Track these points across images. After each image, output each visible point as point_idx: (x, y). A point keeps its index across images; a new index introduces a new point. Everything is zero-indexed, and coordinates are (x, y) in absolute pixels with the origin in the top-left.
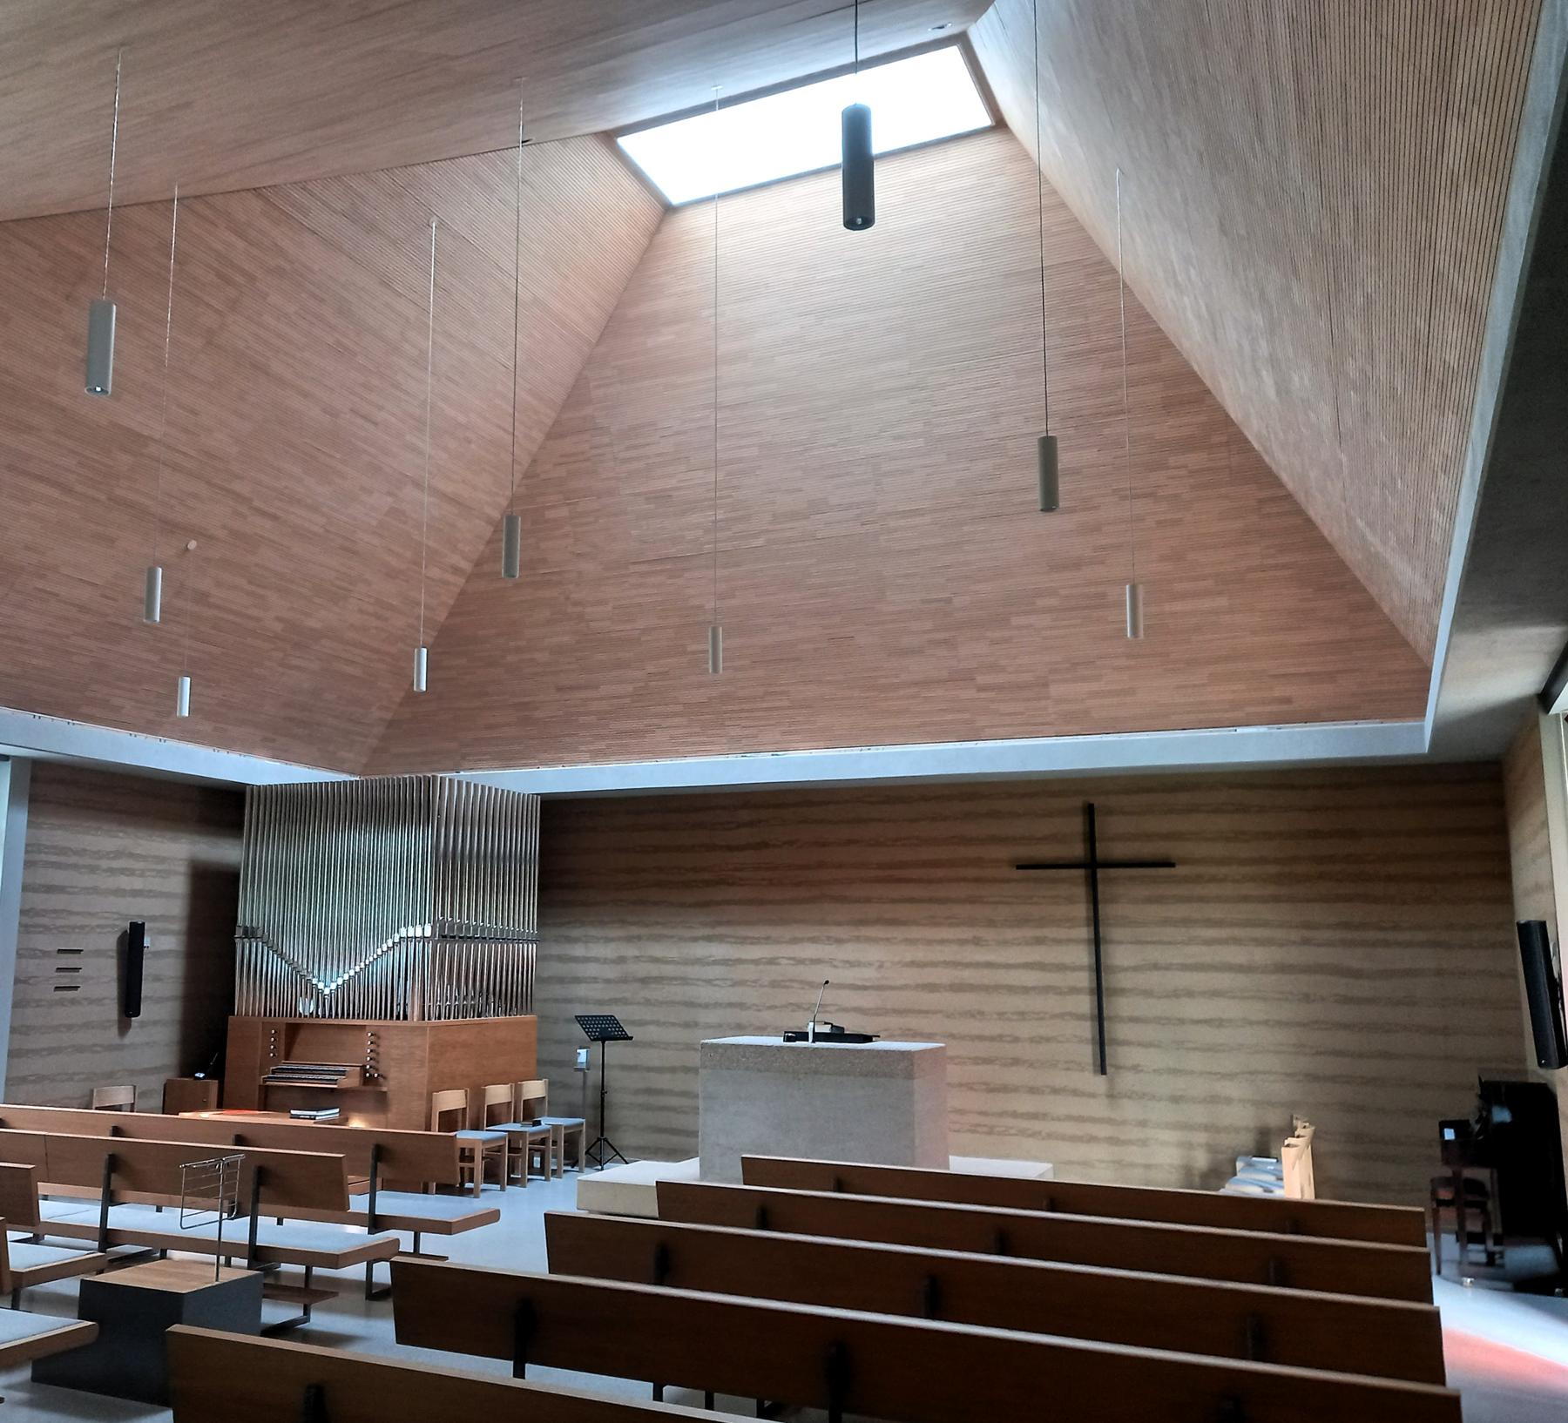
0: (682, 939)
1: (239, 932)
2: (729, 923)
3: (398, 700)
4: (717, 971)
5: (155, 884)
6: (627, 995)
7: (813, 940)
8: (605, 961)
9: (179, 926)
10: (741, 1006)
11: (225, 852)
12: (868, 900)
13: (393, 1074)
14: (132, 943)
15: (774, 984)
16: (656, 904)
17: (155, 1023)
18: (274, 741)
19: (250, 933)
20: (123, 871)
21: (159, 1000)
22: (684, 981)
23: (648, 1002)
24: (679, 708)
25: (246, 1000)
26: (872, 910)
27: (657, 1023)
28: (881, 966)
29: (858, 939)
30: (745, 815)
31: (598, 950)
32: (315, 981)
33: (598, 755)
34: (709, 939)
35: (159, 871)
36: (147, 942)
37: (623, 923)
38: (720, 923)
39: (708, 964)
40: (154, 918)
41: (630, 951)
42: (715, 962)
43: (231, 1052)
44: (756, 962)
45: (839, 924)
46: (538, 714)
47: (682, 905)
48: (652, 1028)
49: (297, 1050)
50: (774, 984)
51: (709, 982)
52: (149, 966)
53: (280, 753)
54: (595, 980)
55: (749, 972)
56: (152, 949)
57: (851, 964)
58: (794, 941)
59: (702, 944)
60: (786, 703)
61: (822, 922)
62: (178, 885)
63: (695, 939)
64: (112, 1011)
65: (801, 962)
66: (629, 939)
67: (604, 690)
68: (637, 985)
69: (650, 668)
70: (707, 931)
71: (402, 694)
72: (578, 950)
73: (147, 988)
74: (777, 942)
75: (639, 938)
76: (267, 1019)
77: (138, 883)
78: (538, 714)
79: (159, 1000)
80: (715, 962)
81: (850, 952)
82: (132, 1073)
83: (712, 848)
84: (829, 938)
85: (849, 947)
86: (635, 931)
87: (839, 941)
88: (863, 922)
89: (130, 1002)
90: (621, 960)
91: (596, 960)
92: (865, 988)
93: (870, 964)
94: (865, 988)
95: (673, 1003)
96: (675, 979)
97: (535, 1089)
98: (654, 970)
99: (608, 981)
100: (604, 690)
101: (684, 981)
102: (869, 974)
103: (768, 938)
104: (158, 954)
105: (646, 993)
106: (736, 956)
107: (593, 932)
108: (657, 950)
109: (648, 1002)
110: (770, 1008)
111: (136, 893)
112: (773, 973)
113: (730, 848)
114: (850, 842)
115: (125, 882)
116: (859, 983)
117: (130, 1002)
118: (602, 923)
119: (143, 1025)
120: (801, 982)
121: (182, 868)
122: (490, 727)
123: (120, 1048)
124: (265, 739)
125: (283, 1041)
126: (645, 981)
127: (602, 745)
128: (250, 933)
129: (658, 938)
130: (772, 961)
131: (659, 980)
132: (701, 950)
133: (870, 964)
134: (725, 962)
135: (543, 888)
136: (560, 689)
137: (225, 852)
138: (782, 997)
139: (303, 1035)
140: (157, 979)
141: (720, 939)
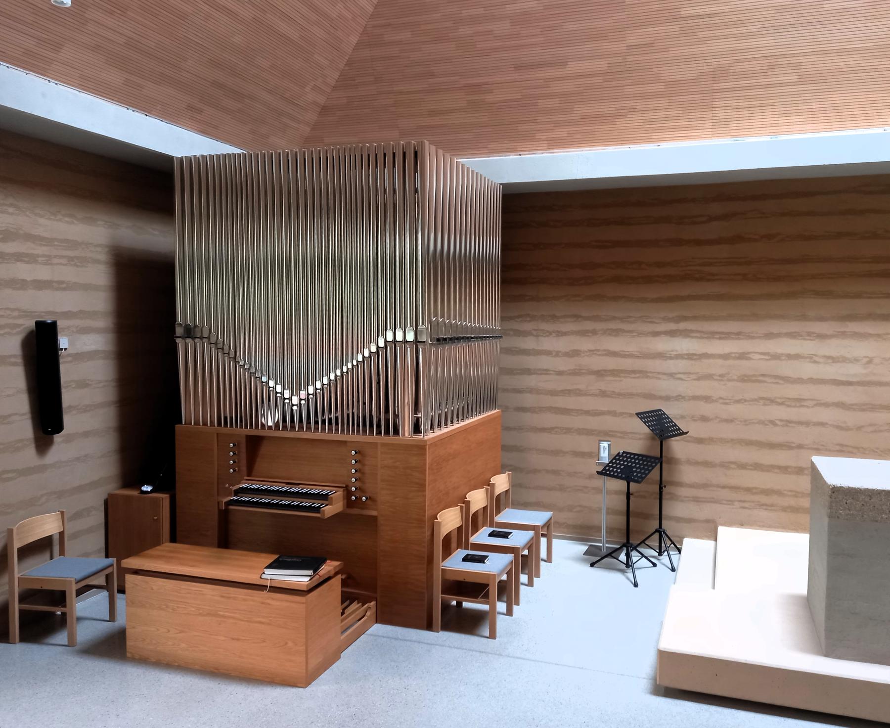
0: (641, 334)
1: (179, 331)
2: (695, 318)
3: (333, 82)
4: (680, 365)
5: (68, 274)
6: (582, 387)
7: (792, 335)
8: (557, 354)
9: (105, 322)
10: (707, 399)
11: (148, 236)
12: (858, 296)
13: (384, 496)
14: (41, 349)
15: (745, 379)
16: (615, 299)
17: (86, 434)
18: (200, 111)
19: (189, 333)
20: (19, 257)
21: (86, 409)
22: (643, 374)
23: (603, 394)
24: (661, 87)
25: (195, 407)
26: (862, 306)
27: (613, 413)
28: (870, 361)
29: (843, 335)
30: (716, 208)
31: (547, 343)
32: (264, 379)
33: (555, 144)
34: (672, 334)
35: (71, 259)
36: (63, 342)
37: (577, 317)
38: (685, 319)
39: (671, 358)
40: (68, 315)
41: (584, 344)
42: (680, 357)
43: (181, 463)
44: (726, 357)
45: (822, 319)
46: (489, 98)
47: (643, 300)
48: (608, 418)
49: (261, 465)
50: (745, 379)
51: (671, 375)
52: (67, 372)
53: (207, 129)
54: (546, 372)
55: (717, 367)
56: (70, 351)
57: (834, 360)
58: (769, 336)
59: (664, 338)
60: (794, 78)
61: (804, 318)
62: (100, 275)
63: (656, 334)
64: (25, 428)
65: (776, 357)
66: (583, 333)
67: (573, 67)
68: (593, 377)
69: (632, 40)
70: (672, 326)
71: (336, 75)
72: (529, 343)
73: (68, 397)
74: (750, 337)
75: (594, 332)
76: (222, 429)
77: (43, 273)
78: (489, 98)
79: (86, 409)
80: (680, 357)
81: (833, 347)
82: (60, 494)
83: (679, 242)
84: (809, 334)
85: (834, 342)
86: (589, 325)
87: (822, 337)
88: (852, 317)
89: (48, 417)
90: (576, 353)
91: (548, 353)
92: (850, 383)
93: (856, 360)
94: (850, 383)
95: (631, 395)
96: (634, 372)
97: (501, 482)
98: (611, 363)
99: (560, 373)
100: (573, 67)
101: (643, 374)
102: (854, 371)
103: (739, 334)
104: (79, 357)
105: (603, 385)
106: (704, 351)
107: (545, 326)
108: (615, 344)
109: (603, 394)
110: (738, 401)
111: (40, 285)
112: (745, 367)
113: (698, 243)
114: (839, 235)
115: (23, 271)
116: (844, 379)
117: (48, 417)
118: (554, 318)
119: (69, 439)
120: (777, 377)
121: (103, 256)
122: (434, 113)
123: (42, 469)
124: (190, 108)
125: (244, 456)
126: (600, 374)
127: (562, 132)
128: (189, 333)
129: (616, 332)
130: (743, 356)
131: (615, 373)
132: (662, 344)
133: (856, 360)
134: (690, 357)
135: (504, 282)
136: (518, 68)
137: (148, 236)
138: (753, 391)
139: (265, 449)
140: (83, 384)
141: (686, 334)
